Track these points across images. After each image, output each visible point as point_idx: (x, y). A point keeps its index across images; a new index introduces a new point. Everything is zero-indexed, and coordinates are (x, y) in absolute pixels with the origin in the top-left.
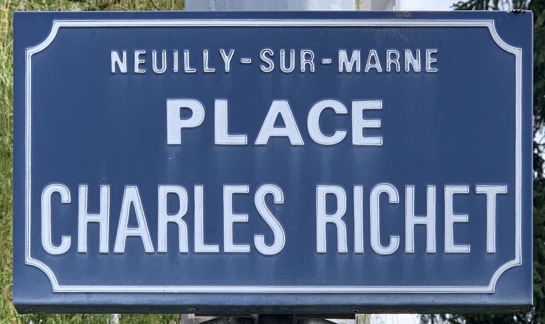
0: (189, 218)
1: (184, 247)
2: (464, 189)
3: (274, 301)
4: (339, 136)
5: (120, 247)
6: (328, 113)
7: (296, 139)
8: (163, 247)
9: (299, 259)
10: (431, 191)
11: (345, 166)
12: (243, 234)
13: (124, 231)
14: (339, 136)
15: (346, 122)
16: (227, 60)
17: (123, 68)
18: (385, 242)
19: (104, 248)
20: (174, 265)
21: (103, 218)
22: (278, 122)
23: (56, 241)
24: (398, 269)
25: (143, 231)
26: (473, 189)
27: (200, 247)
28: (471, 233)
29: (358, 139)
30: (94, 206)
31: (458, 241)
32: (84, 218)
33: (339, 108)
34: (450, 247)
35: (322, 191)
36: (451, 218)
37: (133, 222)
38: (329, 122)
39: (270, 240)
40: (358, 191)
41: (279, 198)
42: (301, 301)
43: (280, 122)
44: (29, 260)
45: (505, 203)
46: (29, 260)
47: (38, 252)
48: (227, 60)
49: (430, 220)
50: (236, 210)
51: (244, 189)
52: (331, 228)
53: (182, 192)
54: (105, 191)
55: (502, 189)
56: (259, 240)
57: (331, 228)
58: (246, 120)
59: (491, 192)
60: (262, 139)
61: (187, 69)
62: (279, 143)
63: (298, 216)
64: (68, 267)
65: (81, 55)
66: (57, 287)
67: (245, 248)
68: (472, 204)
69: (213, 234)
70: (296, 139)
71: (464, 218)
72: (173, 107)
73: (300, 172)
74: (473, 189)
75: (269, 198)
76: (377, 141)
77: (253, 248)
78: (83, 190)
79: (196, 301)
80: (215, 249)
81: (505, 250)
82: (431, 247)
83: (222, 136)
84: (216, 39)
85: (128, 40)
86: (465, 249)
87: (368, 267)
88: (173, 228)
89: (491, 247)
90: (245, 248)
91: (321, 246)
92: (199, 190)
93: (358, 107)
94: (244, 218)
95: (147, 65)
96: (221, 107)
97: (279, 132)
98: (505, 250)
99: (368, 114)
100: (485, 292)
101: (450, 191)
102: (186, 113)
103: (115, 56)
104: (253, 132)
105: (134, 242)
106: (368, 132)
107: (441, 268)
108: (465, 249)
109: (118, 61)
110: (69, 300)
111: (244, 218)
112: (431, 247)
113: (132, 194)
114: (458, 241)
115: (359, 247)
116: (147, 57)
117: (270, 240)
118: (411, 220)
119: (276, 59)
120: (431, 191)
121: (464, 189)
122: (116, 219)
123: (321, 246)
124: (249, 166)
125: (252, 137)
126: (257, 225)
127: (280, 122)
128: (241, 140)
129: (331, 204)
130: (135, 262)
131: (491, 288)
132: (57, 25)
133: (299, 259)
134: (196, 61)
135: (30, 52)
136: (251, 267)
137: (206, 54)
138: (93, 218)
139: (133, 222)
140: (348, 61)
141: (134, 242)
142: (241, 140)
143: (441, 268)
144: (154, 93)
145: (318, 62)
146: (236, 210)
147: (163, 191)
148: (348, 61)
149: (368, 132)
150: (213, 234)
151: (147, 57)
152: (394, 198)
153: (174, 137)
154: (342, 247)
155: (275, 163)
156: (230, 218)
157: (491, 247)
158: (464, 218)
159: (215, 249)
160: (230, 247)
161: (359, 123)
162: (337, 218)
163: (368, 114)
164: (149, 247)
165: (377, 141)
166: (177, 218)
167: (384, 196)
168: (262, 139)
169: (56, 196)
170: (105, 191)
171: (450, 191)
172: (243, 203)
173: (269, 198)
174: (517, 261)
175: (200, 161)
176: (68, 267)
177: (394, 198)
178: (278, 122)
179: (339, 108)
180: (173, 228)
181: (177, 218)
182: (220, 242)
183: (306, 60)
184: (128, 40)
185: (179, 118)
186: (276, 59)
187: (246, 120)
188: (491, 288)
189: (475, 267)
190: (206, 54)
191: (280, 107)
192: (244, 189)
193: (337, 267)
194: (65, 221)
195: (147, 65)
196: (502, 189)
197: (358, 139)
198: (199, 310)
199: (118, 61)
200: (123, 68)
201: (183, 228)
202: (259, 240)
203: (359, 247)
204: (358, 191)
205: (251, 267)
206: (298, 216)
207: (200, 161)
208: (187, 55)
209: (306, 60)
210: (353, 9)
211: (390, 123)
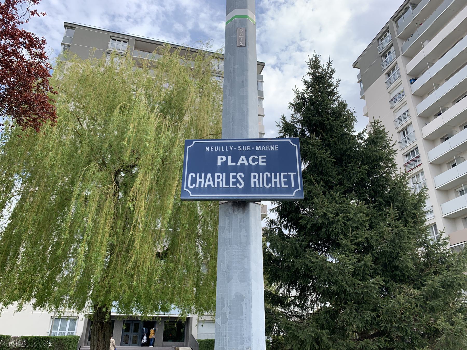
0: (222, 180)
1: (221, 186)
2: (286, 174)
3: (241, 198)
4: (256, 163)
5: (206, 186)
6: (253, 159)
7: (246, 164)
8: (216, 186)
9: (247, 189)
10: (278, 174)
11: (258, 169)
12: (234, 183)
13: (207, 183)
14: (256, 163)
15: (258, 160)
16: (231, 148)
17: (208, 150)
18: (267, 185)
19: (202, 186)
20: (218, 190)
21: (202, 180)
22: (243, 160)
23: (192, 185)
24: (271, 191)
25: (211, 183)
26: (288, 174)
27: (224, 186)
28: (288, 183)
29: (260, 163)
30: (200, 178)
31: (285, 185)
32: (198, 180)
33: (256, 157)
34: (283, 186)
35: (252, 174)
36: (283, 180)
37: (209, 181)
38: (254, 160)
39: (241, 185)
40: (261, 174)
41: (243, 176)
42: (248, 198)
43: (243, 160)
44: (185, 189)
45: (296, 177)
46: (185, 189)
47: (187, 187)
48: (231, 148)
49: (278, 180)
50: (233, 178)
51: (235, 174)
52: (255, 182)
53: (221, 175)
54: (203, 175)
55: (295, 174)
56: (238, 185)
57: (255, 182)
58: (235, 160)
59: (292, 174)
60: (239, 164)
61: (222, 150)
62: (243, 165)
63: (247, 180)
64: (194, 191)
65: (199, 148)
66: (191, 195)
67: (235, 186)
68: (288, 177)
69: (228, 183)
70: (246, 164)
71: (286, 180)
72: (219, 157)
73: (247, 171)
74: (288, 174)
75: (240, 176)
76: (265, 164)
77: (237, 186)
78: (198, 175)
79: (223, 198)
80: (228, 186)
81: (296, 187)
82: (278, 186)
83: (230, 163)
84: (229, 144)
85: (209, 145)
86: (287, 186)
87: (264, 190)
88: (218, 182)
89: (293, 186)
90: (235, 186)
91: (253, 186)
92: (224, 174)
93: (260, 157)
94: (235, 180)
95: (214, 149)
96: (230, 157)
97: (243, 162)
98: (296, 187)
99: (262, 158)
100: (292, 196)
101: (282, 174)
102: (222, 159)
103: (207, 148)
104: (237, 162)
105: (209, 185)
106: (263, 162)
107: (281, 191)
108: (287, 186)
109: (207, 149)
110: (193, 198)
111: (235, 180)
112: (278, 186)
113: (209, 175)
114: (285, 185)
115: (261, 186)
116: (214, 148)
117: (241, 185)
118: (273, 180)
119: (242, 148)
120: (278, 174)
121: (286, 174)
122: (205, 180)
123: (253, 186)
124: (236, 169)
125: (237, 163)
126: (238, 181)
127: (243, 160)
128: (234, 164)
129: (255, 177)
130: (209, 190)
131: (293, 195)
132: (194, 142)
133: (247, 189)
134: (224, 148)
135: (188, 147)
136: (236, 190)
137: (226, 147)
138: (200, 180)
139: (209, 181)
140: (258, 148)
141: (209, 185)
142: (234, 164)
143: (281, 191)
144: (214, 155)
145: (251, 148)
146: (233, 178)
147: (216, 174)
148: (258, 148)
149: (263, 162)
150: (228, 183)
151: (214, 148)
152: (269, 175)
153: (219, 163)
154: (257, 186)
155: (242, 168)
156: (231, 180)
157: (293, 186)
158: (286, 180)
159: (228, 186)
160: (231, 186)
161: (260, 160)
162: (256, 180)
163: (262, 158)
164: (213, 186)
165: (265, 164)
166: (219, 180)
167: (267, 175)
168: (239, 164)
169: (192, 176)
170: (203, 175)
171: (282, 174)
172: (234, 177)
173: (240, 176)
174: (300, 189)
175: (225, 168)
176: (194, 191)
177: (269, 175)
178: (243, 160)
179: (256, 157)
180: (218, 182)
181: (219, 180)
182: (229, 185)
183: (249, 148)
184: (209, 145)
185: (220, 160)
186: (242, 148)
187: (235, 160)
188: (293, 195)
189: (289, 190)
190: (226, 147)
191: (243, 157)
192: (235, 174)
193: (256, 190)
194: (194, 181)
195: (214, 149)
196: (295, 174)
197: (260, 163)
198: (224, 200)
199: (207, 149)
200: (208, 150)
201: (221, 182)
202: (238, 185)
203: (261, 186)
204: (261, 174)
205: (236, 190)
206: (247, 180)
207: (225, 168)
208: (222, 147)
209: (249, 148)
210: (258, 138)
211: (268, 160)
